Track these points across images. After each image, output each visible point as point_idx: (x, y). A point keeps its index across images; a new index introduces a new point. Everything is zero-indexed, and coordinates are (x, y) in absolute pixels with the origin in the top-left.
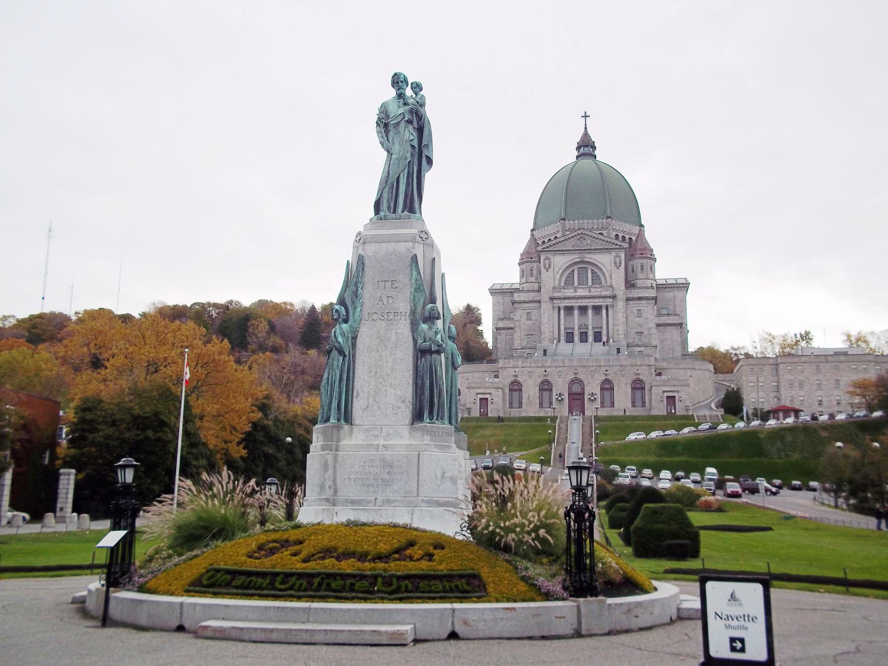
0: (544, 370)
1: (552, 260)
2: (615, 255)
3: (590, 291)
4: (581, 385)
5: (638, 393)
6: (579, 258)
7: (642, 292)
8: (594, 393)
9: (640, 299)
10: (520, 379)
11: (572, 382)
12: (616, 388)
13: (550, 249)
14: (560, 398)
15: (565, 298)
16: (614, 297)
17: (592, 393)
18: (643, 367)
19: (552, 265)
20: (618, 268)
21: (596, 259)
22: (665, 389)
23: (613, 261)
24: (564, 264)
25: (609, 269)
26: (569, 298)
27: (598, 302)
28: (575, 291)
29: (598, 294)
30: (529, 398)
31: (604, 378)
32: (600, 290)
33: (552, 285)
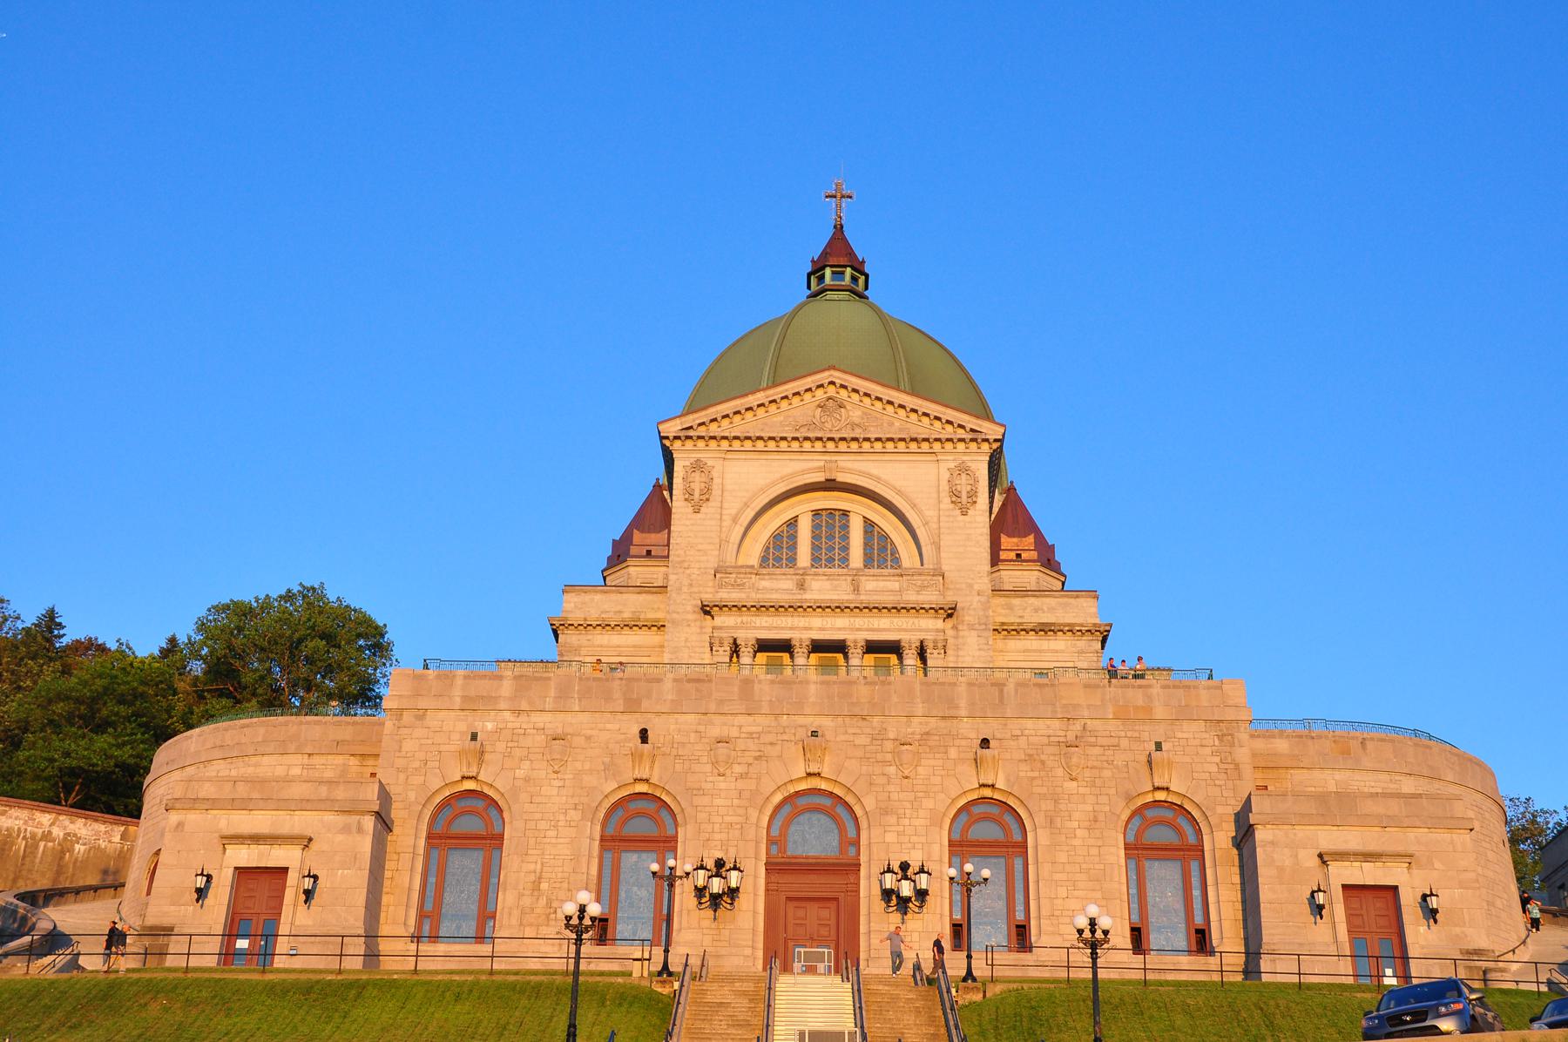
0: (636, 730)
1: (715, 474)
2: (952, 465)
3: (856, 590)
4: (835, 819)
5: (1164, 878)
6: (819, 470)
7: (1052, 609)
8: (915, 866)
9: (1044, 629)
10: (494, 778)
11: (796, 804)
12: (1037, 838)
13: (714, 429)
14: (716, 885)
15: (761, 608)
16: (950, 613)
17: (905, 867)
18: (1190, 731)
19: (716, 492)
20: (964, 514)
21: (884, 477)
22: (1330, 839)
23: (945, 486)
24: (763, 490)
25: (931, 514)
26: (778, 608)
27: (885, 628)
28: (801, 586)
29: (889, 599)
30: (536, 886)
31: (966, 784)
32: (896, 586)
33: (713, 563)
